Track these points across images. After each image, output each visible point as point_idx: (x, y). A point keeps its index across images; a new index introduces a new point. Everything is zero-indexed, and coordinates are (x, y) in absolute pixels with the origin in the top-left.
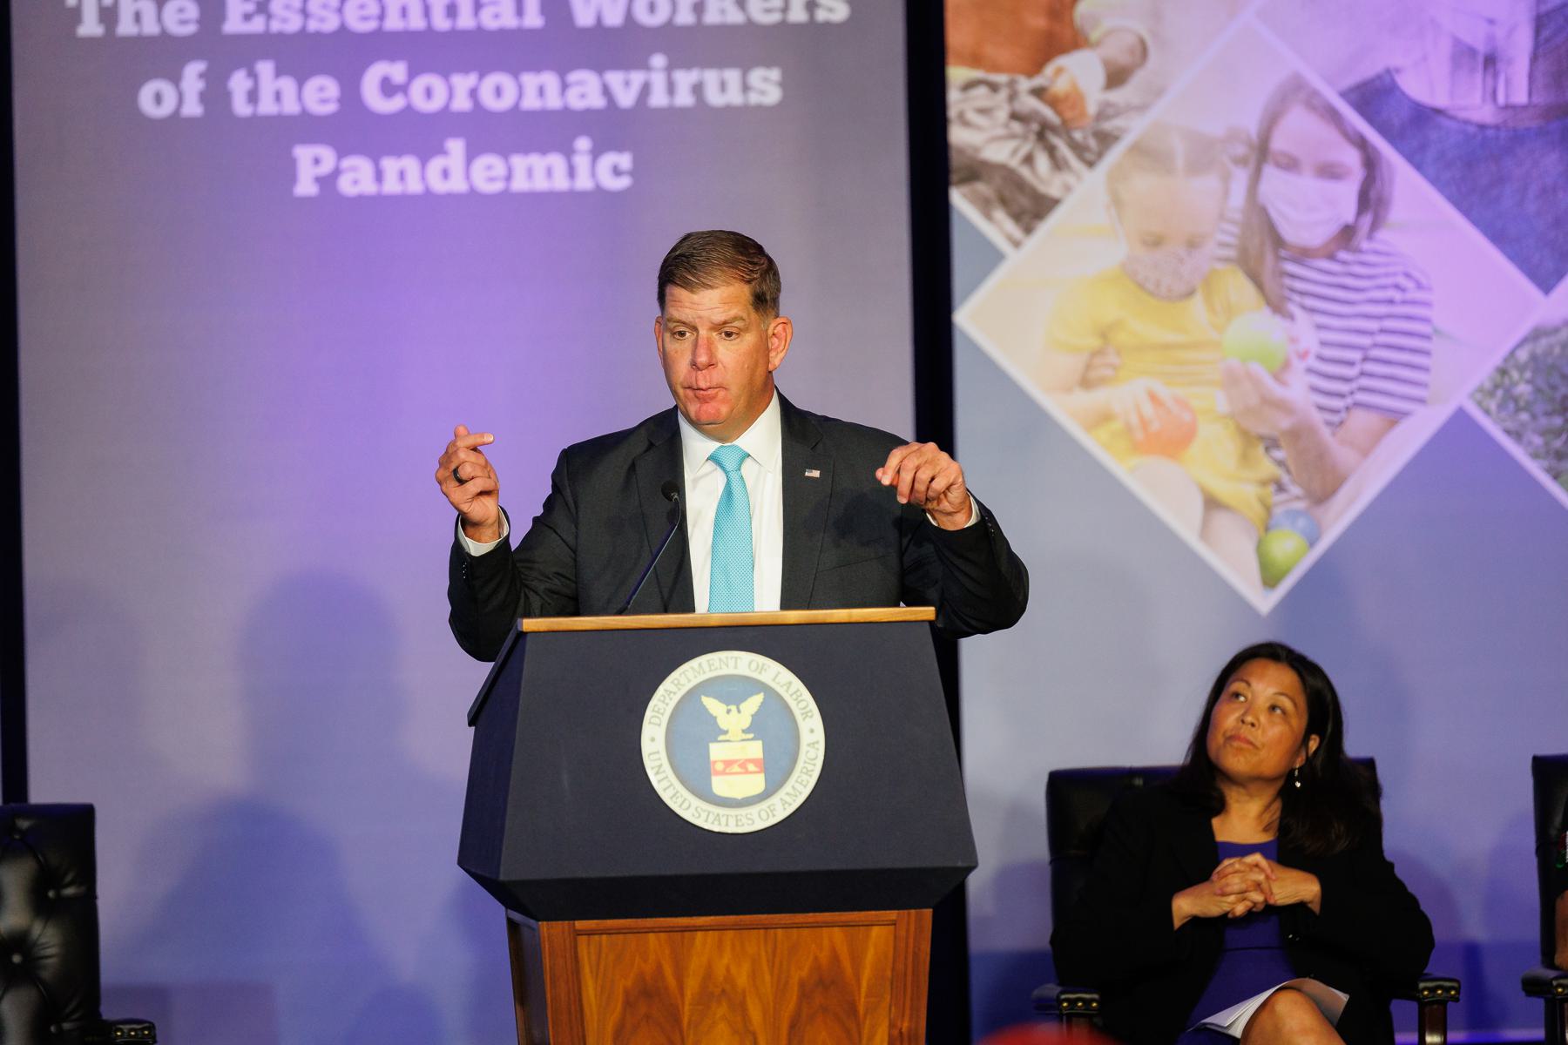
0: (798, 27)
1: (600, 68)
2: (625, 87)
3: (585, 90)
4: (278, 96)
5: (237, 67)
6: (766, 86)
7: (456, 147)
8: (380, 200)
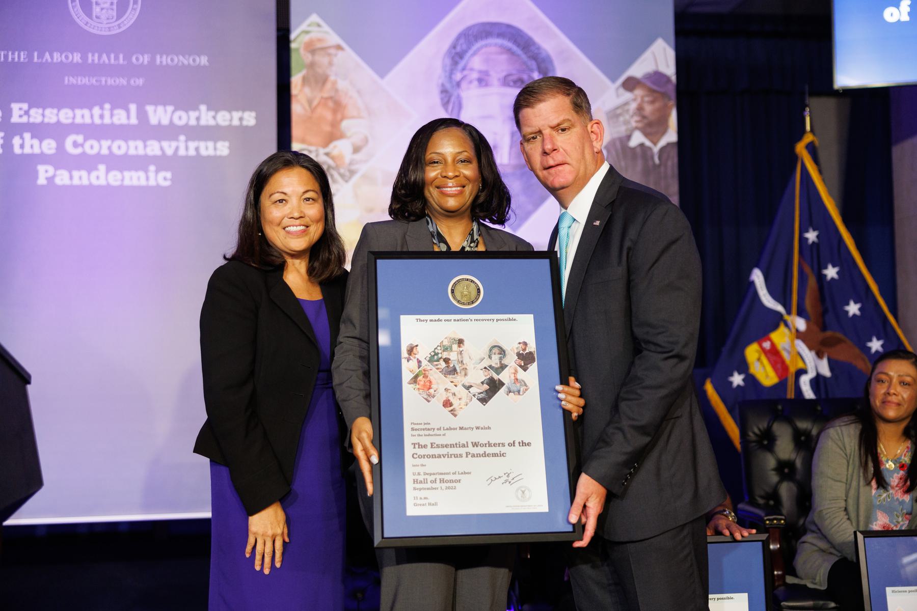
0: (236, 127)
1: (159, 139)
2: (169, 148)
3: (154, 148)
4: (32, 146)
5: (16, 135)
6: (223, 148)
7: (102, 168)
8: (72, 187)
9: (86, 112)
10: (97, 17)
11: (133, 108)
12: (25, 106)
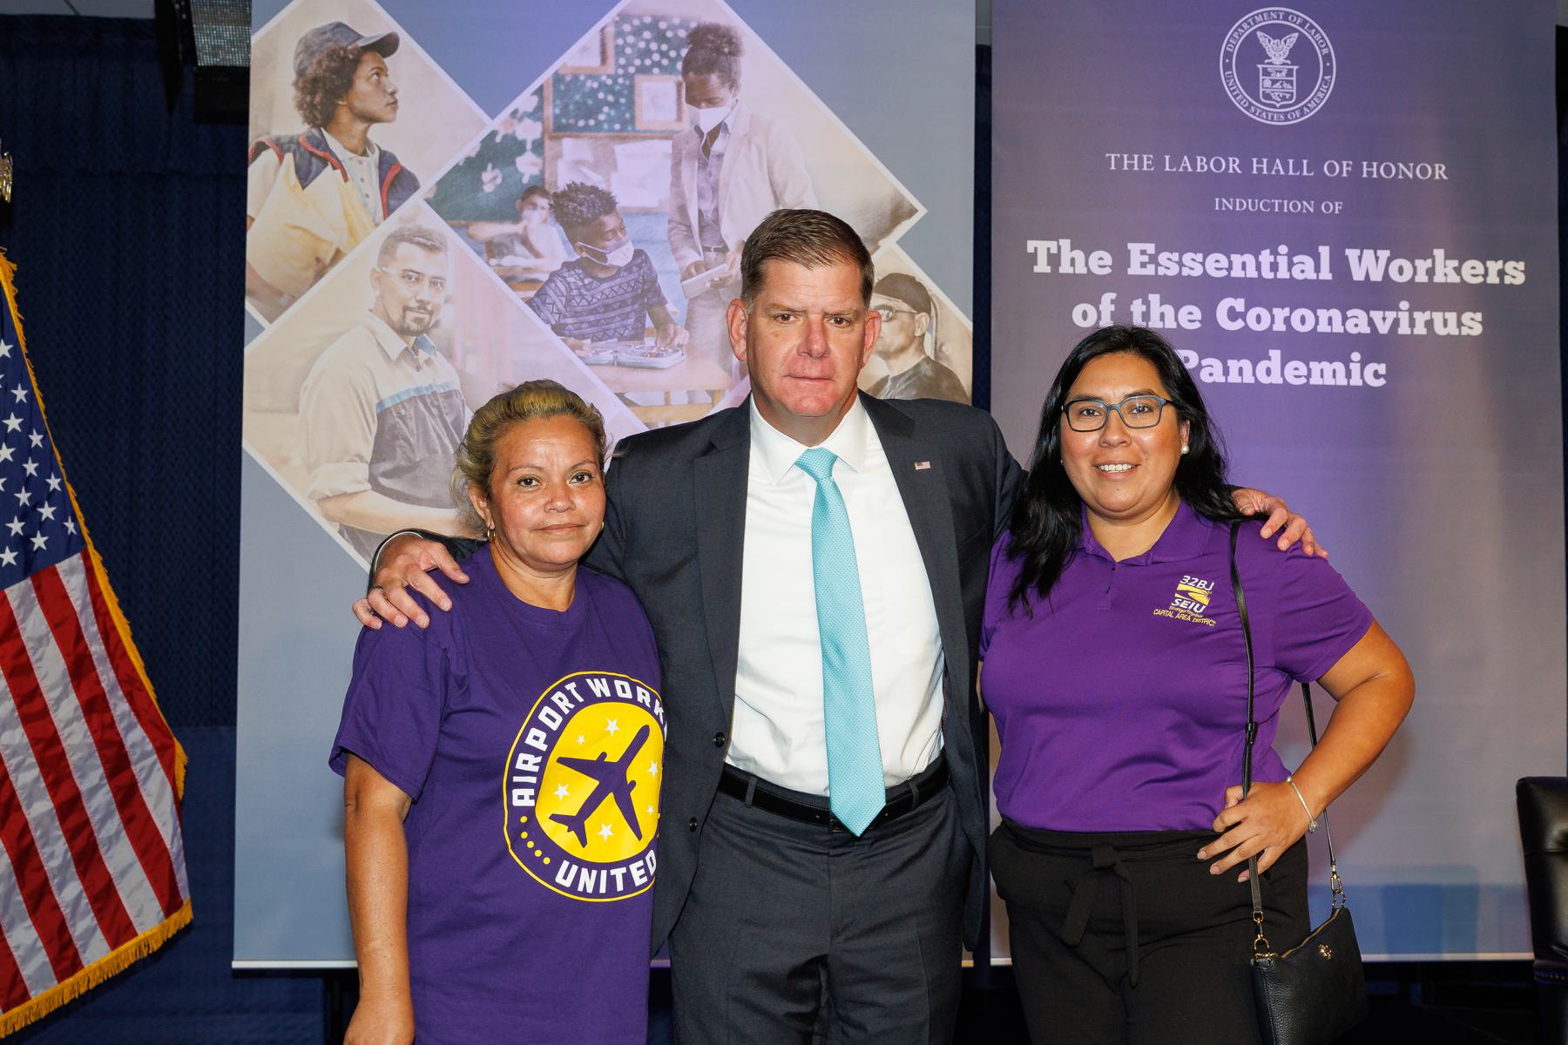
3: (1358, 322)
4: (1162, 316)
6: (1473, 324)
7: (1275, 354)
9: (1249, 259)
10: (1267, 96)
11: (1324, 251)
12: (1150, 248)
